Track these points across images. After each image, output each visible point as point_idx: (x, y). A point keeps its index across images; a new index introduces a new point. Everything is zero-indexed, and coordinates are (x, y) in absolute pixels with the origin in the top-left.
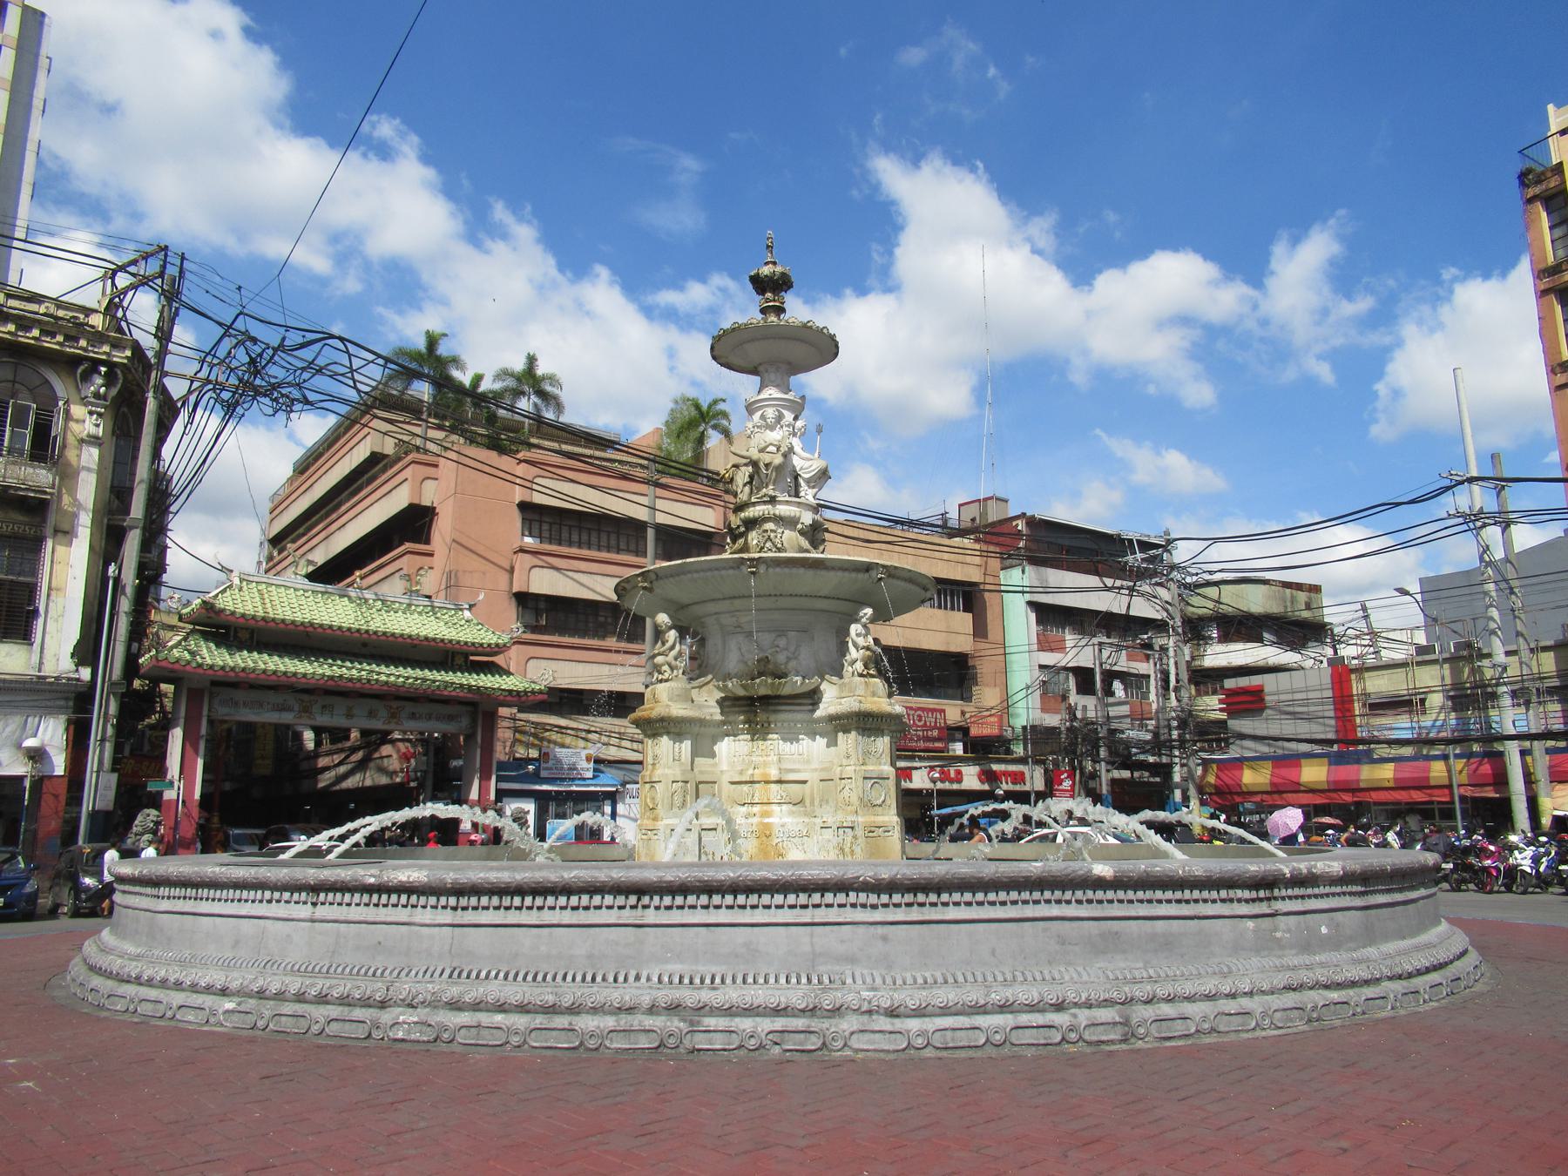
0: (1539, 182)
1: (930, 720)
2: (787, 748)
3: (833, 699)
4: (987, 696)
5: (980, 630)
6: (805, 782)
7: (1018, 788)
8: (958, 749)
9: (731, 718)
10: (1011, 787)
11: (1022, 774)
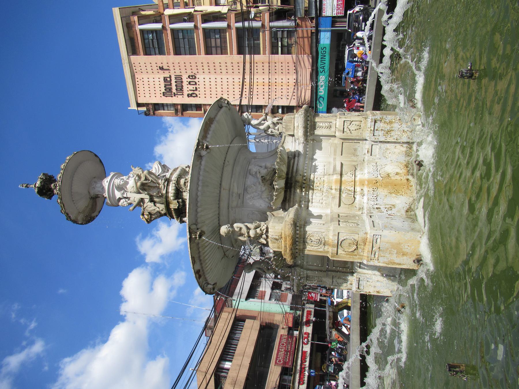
0: (149, 111)
1: (284, 341)
2: (320, 170)
3: (293, 145)
4: (278, 319)
5: (253, 318)
6: (342, 164)
7: (313, 314)
8: (296, 333)
9: (297, 198)
10: (312, 316)
11: (308, 311)
